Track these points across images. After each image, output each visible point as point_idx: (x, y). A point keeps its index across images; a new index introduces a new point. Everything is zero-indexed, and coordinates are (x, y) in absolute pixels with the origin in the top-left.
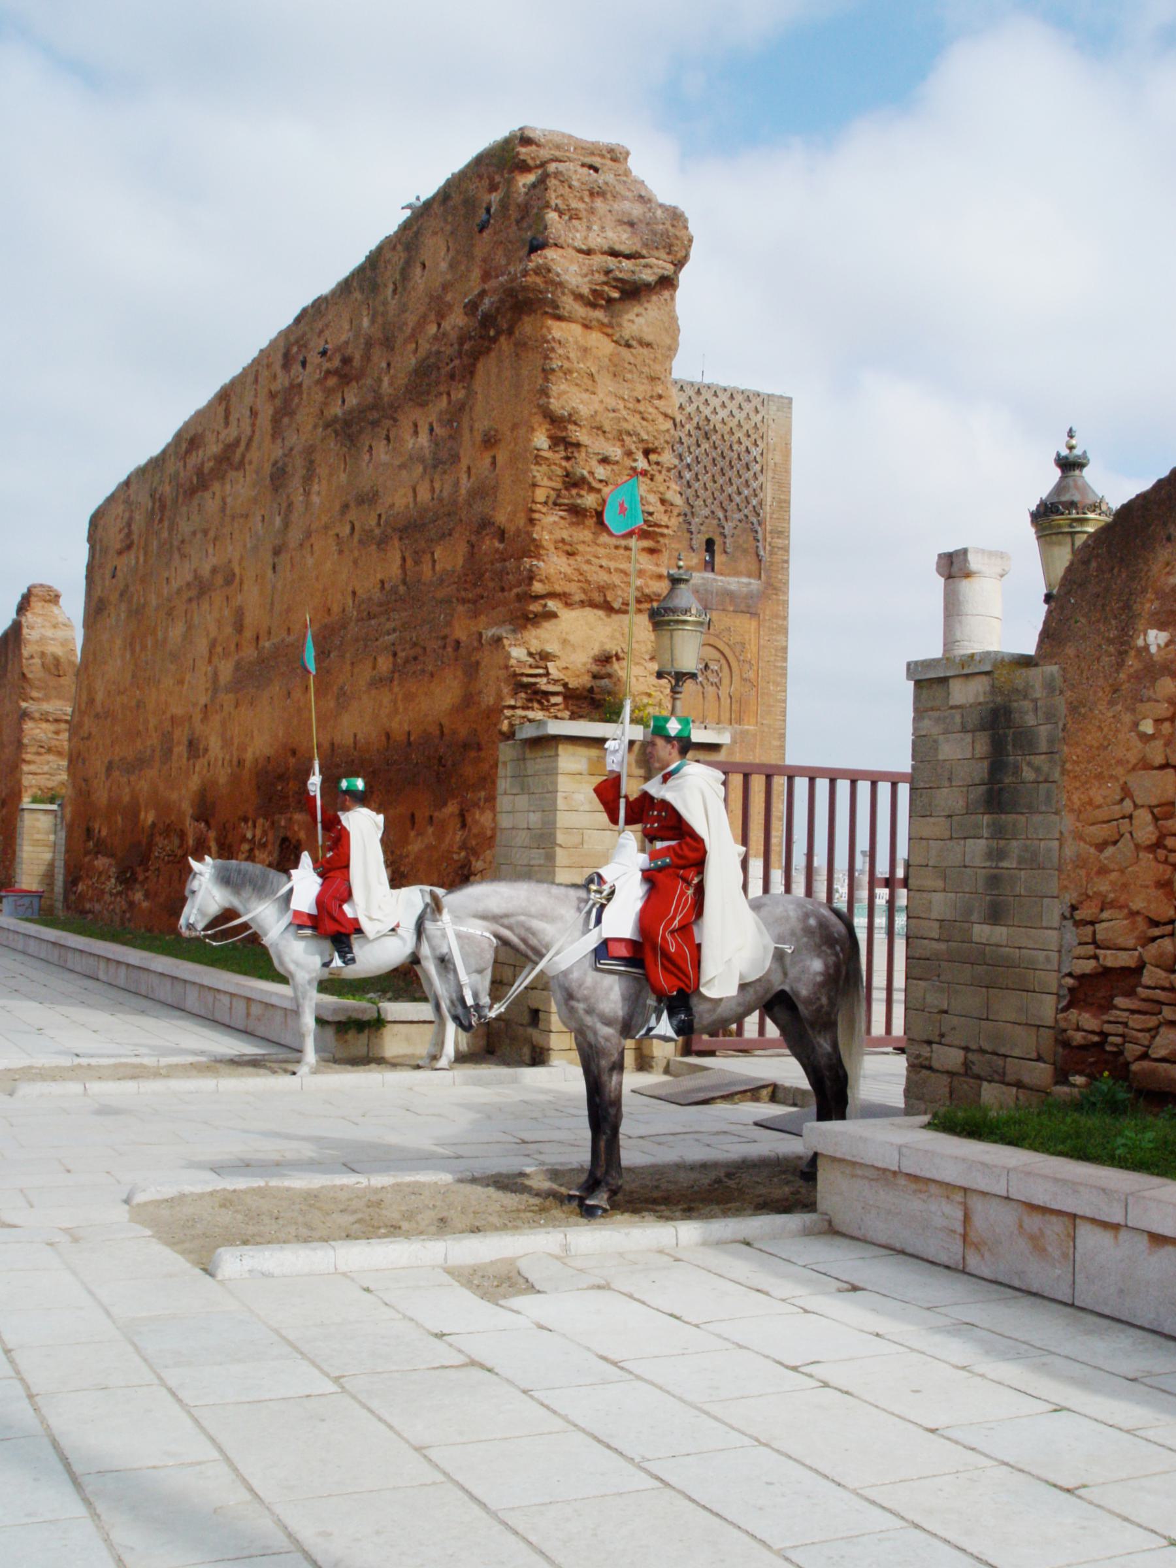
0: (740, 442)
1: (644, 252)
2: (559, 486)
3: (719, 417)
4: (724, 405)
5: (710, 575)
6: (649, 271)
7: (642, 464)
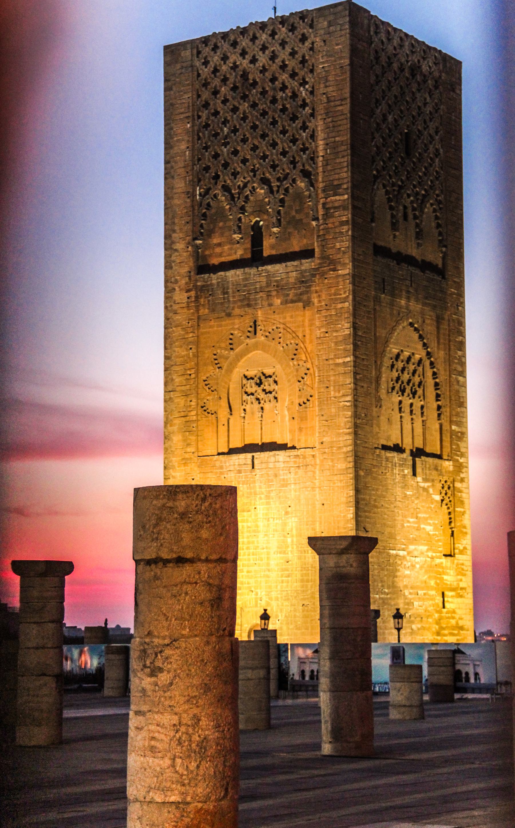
0: (284, 88)
4: (264, 48)
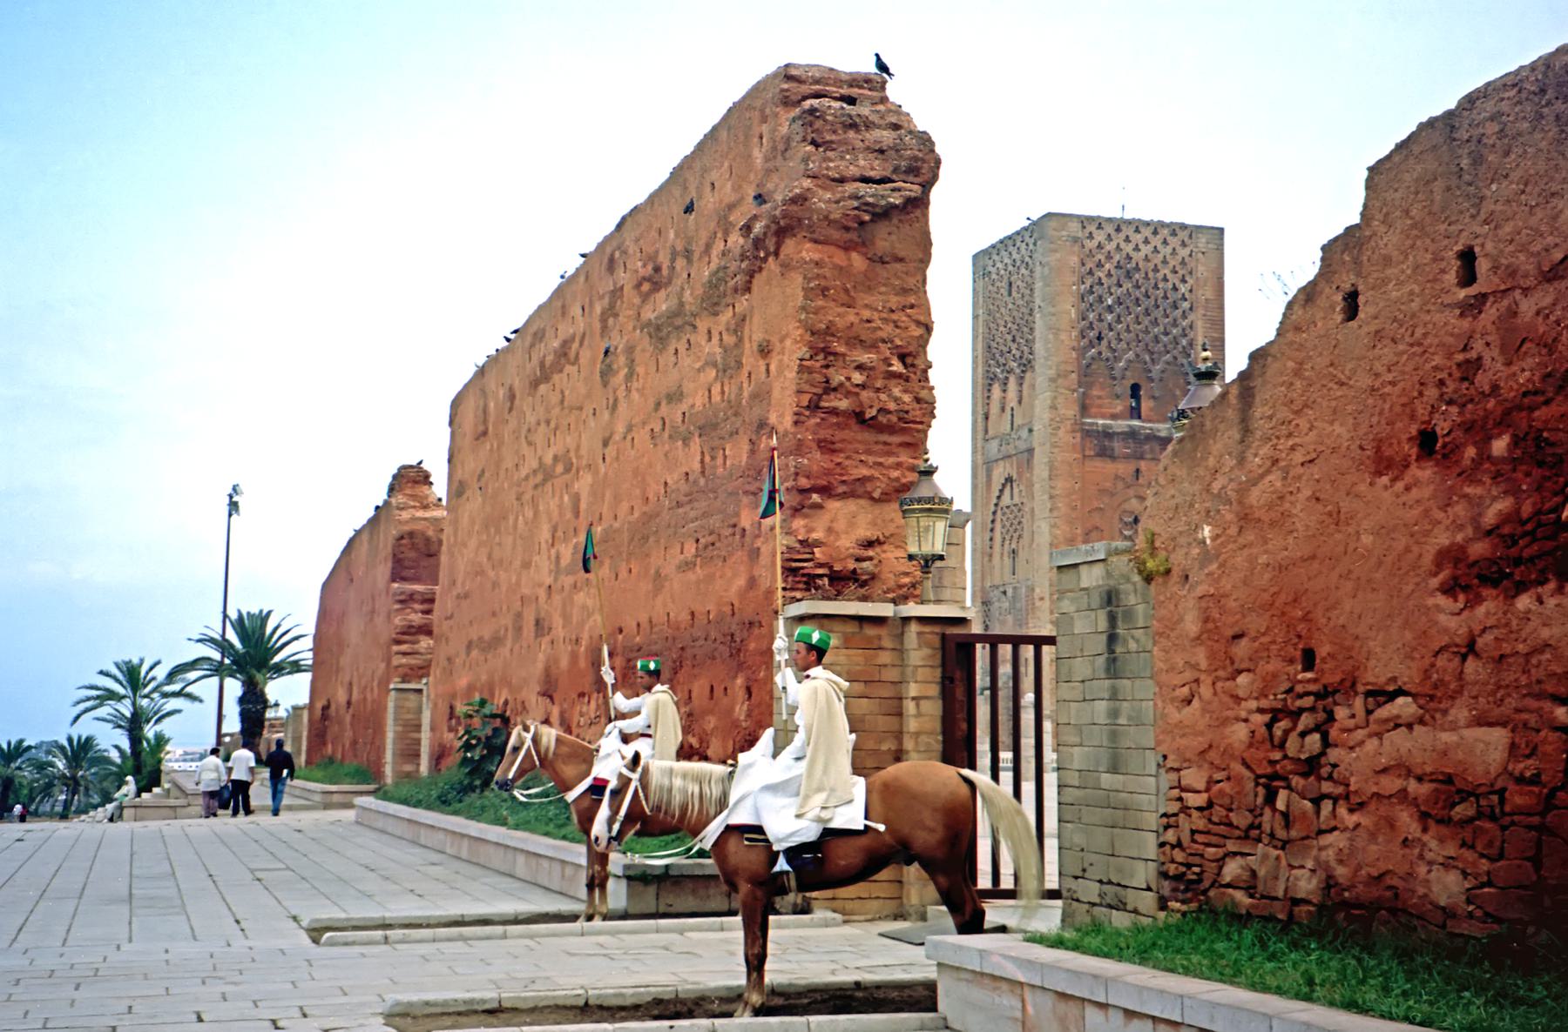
0: (1165, 279)
1: (894, 177)
2: (819, 391)
3: (1142, 254)
4: (1146, 241)
5: (1136, 423)
6: (896, 194)
7: (897, 367)
